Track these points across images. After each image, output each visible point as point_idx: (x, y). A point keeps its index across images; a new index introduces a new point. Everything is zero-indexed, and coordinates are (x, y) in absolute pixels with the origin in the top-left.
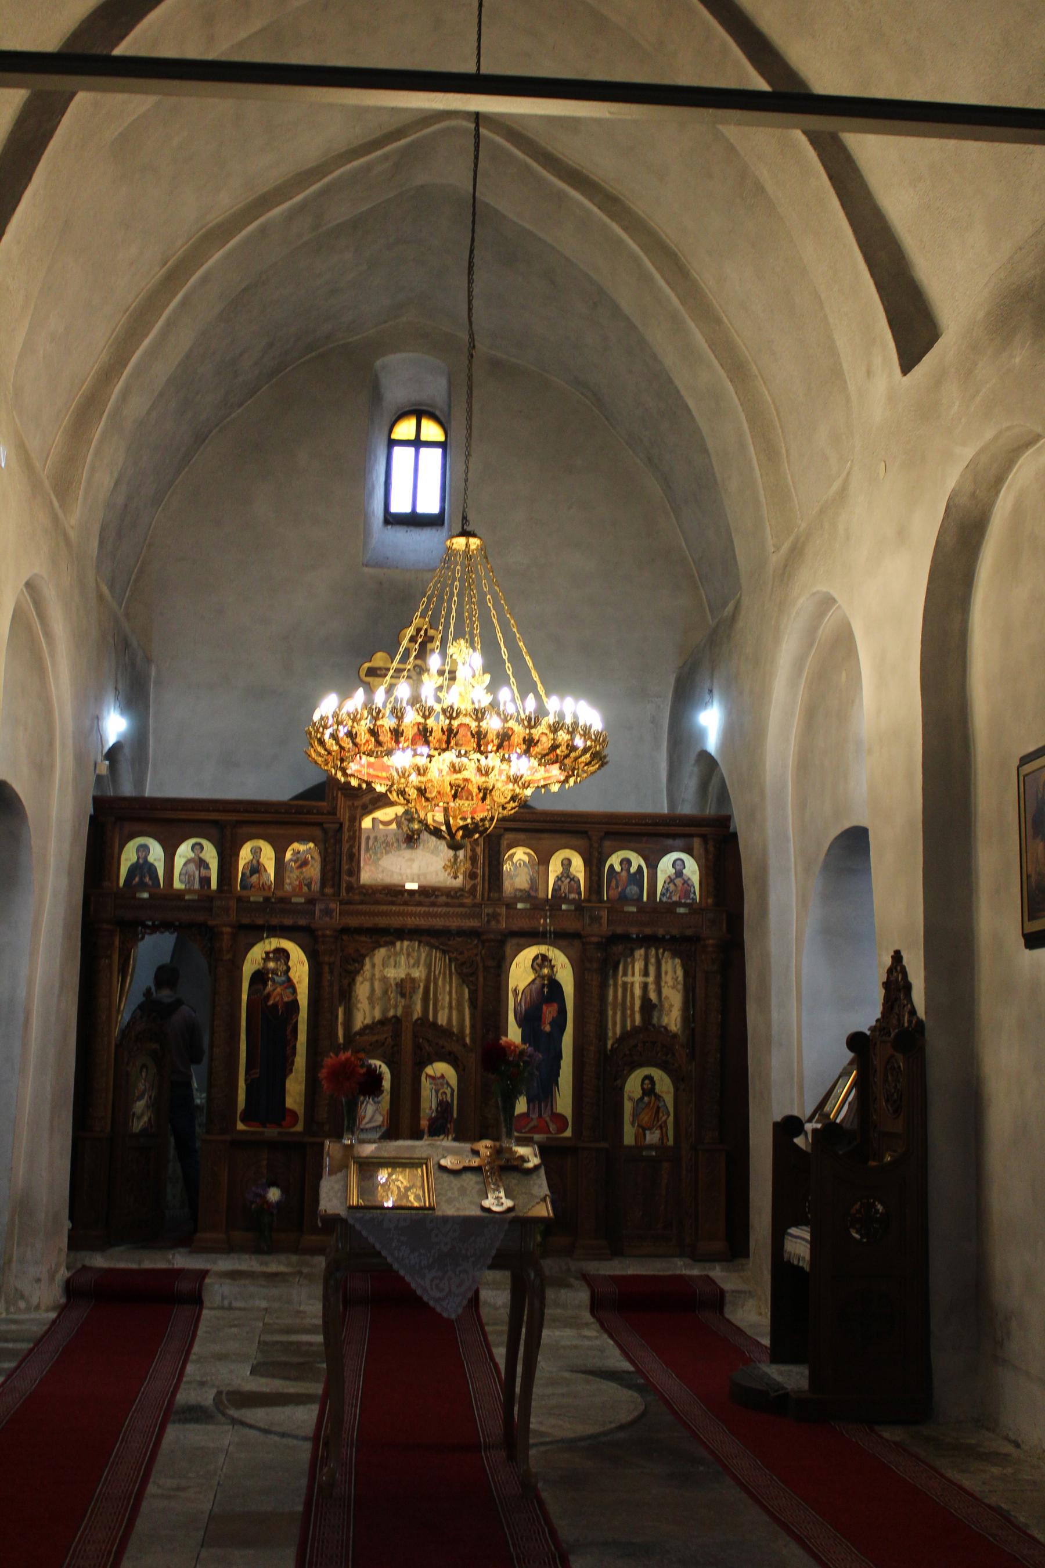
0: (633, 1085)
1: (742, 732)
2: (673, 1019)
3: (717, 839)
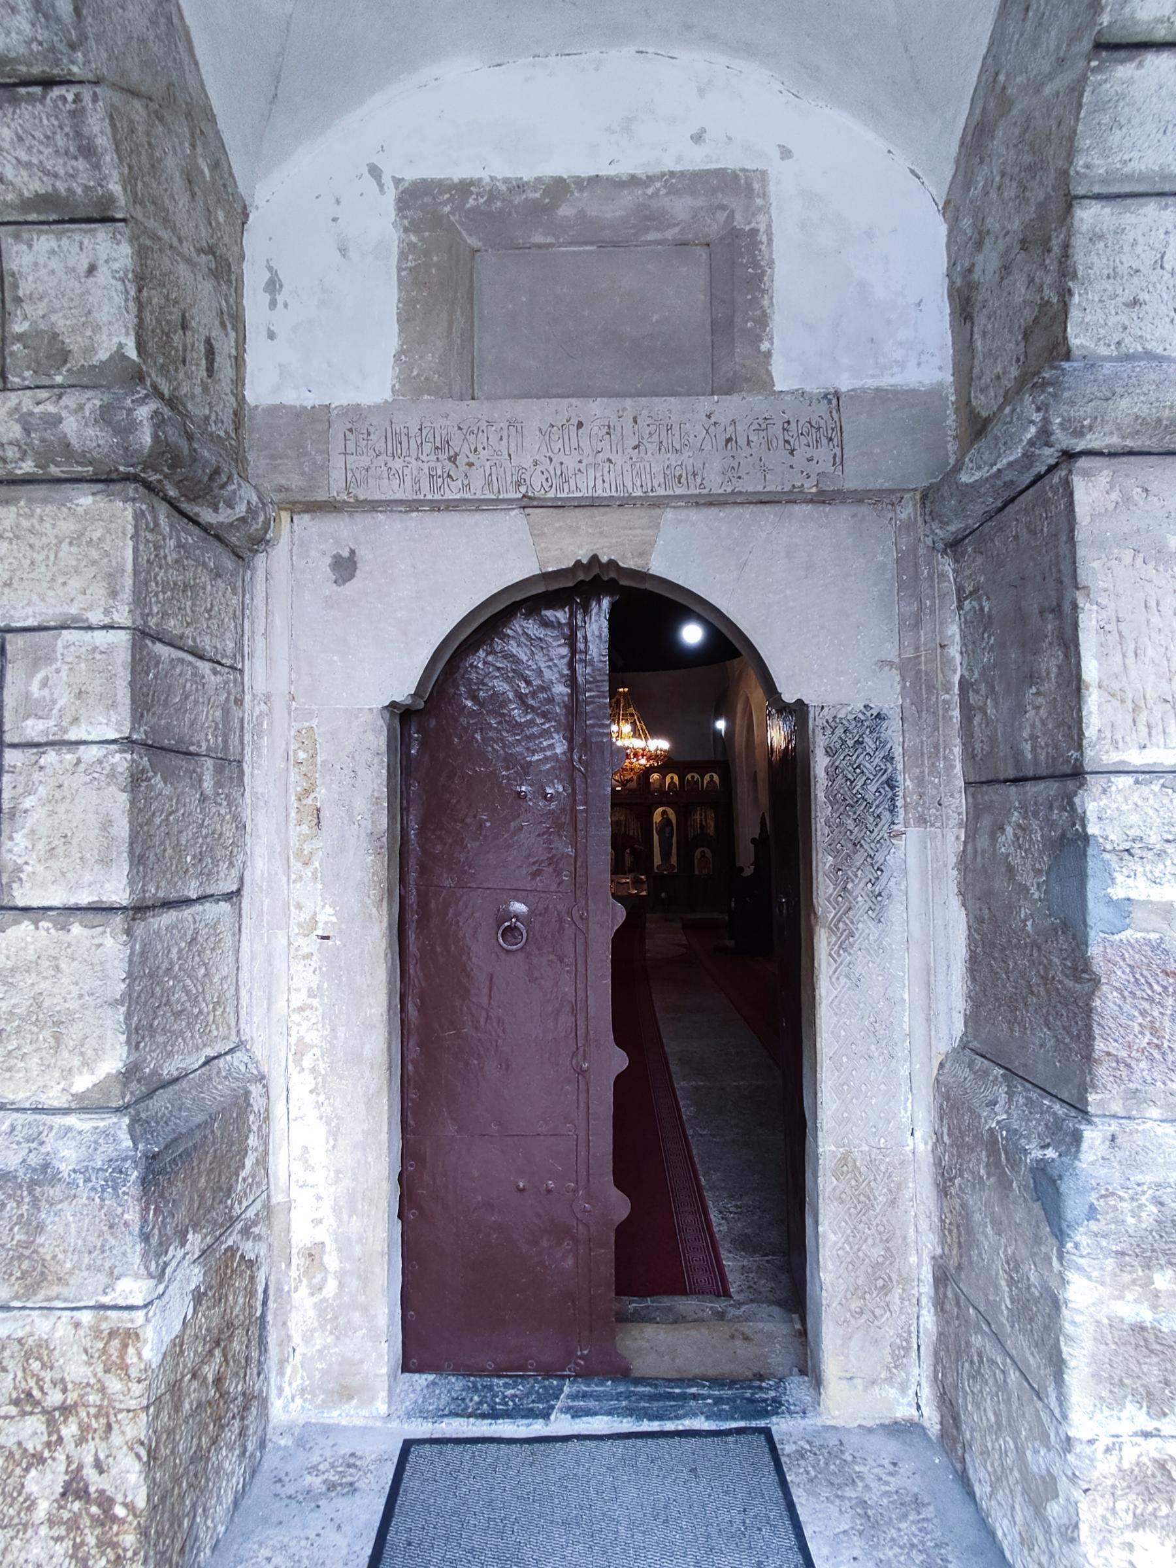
0: (698, 853)
1: (730, 730)
2: (711, 830)
3: (724, 767)
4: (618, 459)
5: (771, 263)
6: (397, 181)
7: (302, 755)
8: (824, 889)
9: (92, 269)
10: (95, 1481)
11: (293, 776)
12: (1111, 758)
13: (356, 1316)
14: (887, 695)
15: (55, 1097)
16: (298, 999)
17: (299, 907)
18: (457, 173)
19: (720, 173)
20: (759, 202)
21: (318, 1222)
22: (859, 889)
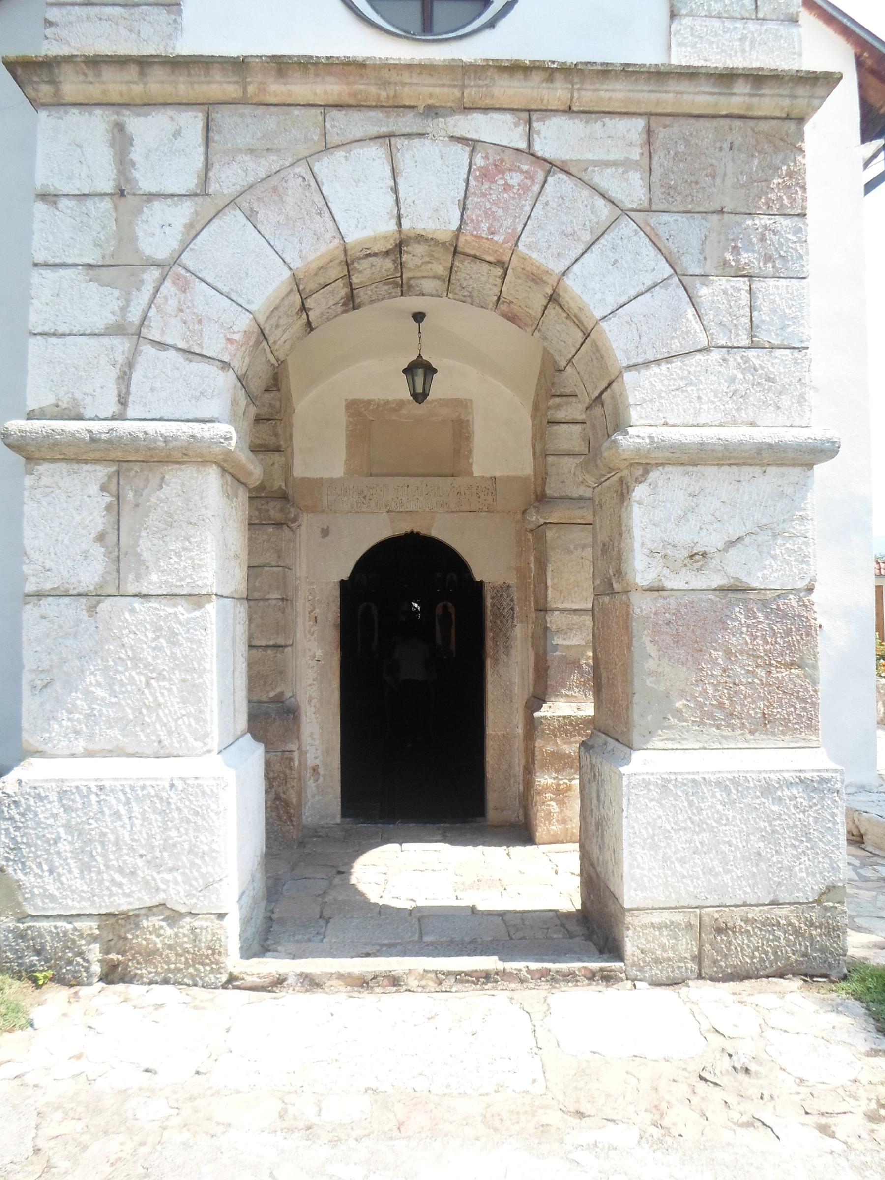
4: (421, 498)
5: (473, 432)
6: (346, 400)
7: (310, 598)
8: (489, 644)
9: (273, 464)
10: (283, 796)
11: (308, 605)
12: (554, 606)
13: (330, 790)
14: (512, 579)
15: (264, 699)
16: (310, 682)
17: (309, 650)
18: (366, 398)
19: (456, 399)
20: (470, 410)
21: (316, 758)
22: (501, 645)
